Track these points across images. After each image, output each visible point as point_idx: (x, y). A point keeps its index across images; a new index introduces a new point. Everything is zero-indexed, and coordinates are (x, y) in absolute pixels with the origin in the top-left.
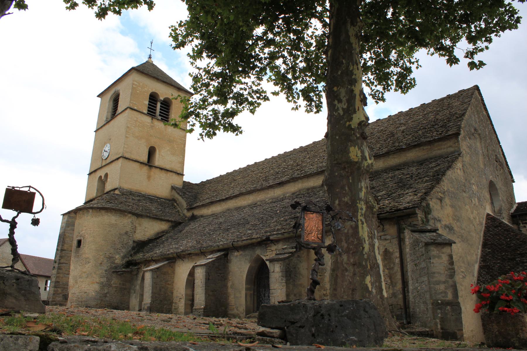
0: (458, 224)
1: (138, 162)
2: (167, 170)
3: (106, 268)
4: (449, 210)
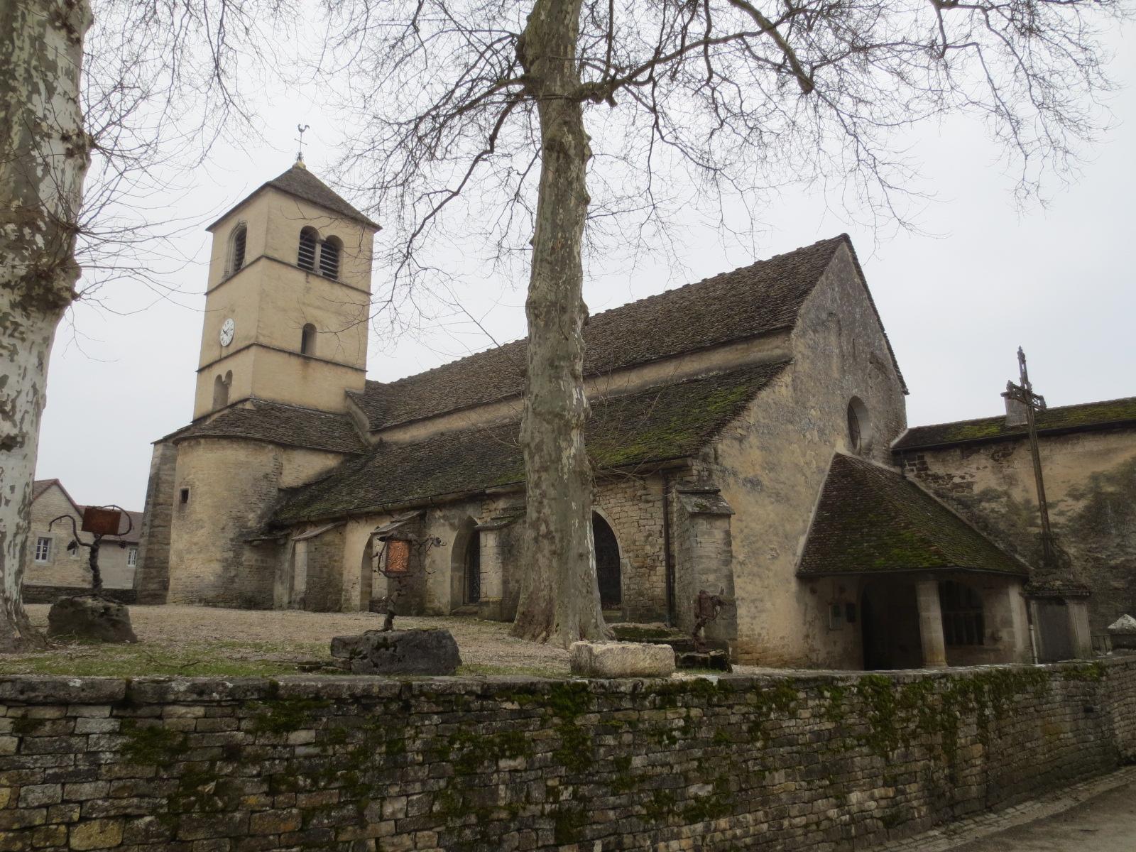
0: (771, 475)
1: (285, 352)
2: (336, 364)
3: (232, 536)
4: (756, 455)
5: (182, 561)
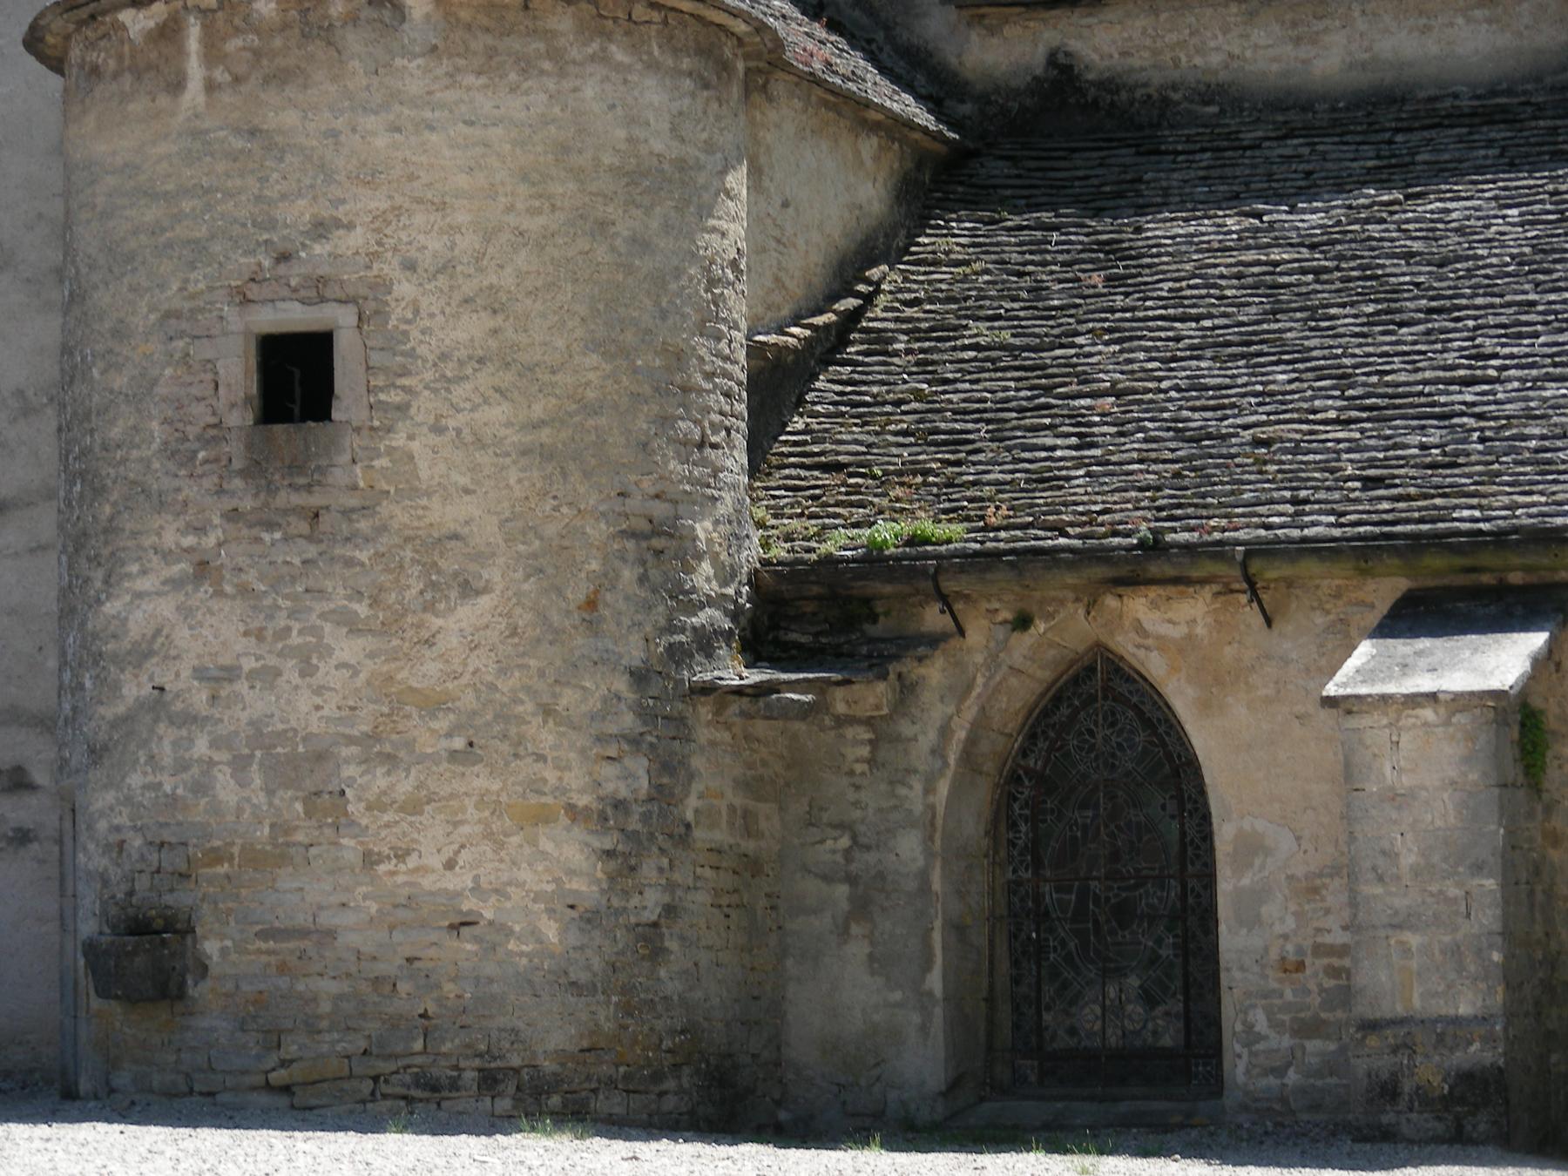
3: (634, 652)
5: (328, 805)
